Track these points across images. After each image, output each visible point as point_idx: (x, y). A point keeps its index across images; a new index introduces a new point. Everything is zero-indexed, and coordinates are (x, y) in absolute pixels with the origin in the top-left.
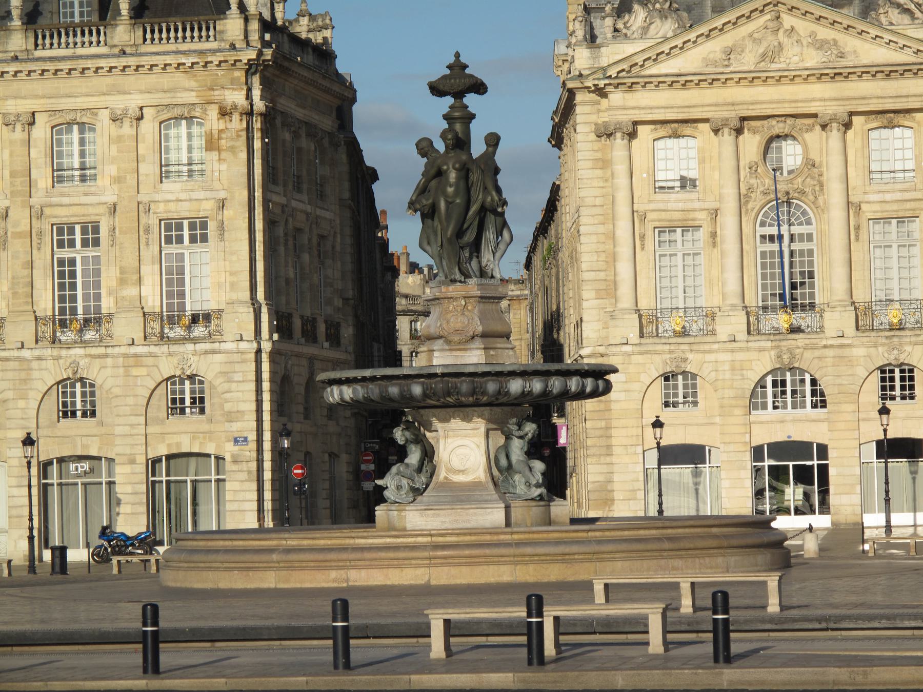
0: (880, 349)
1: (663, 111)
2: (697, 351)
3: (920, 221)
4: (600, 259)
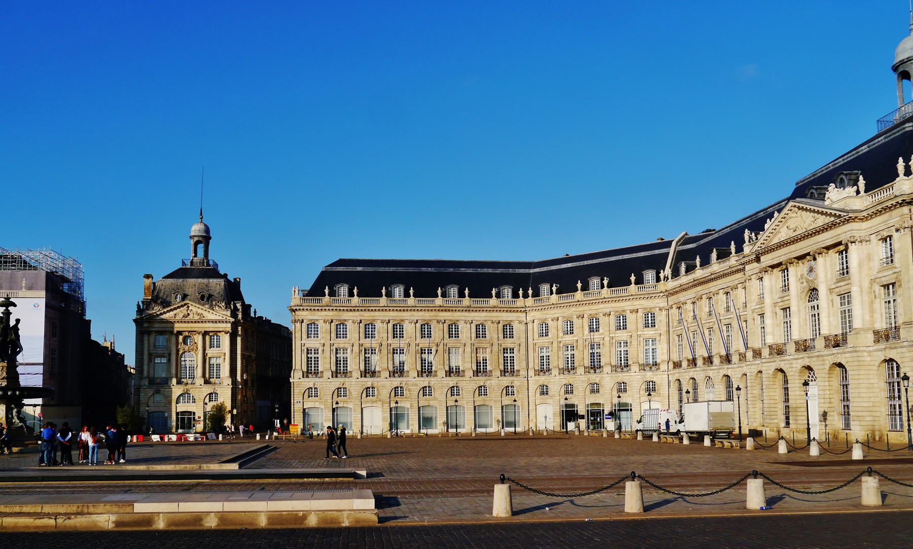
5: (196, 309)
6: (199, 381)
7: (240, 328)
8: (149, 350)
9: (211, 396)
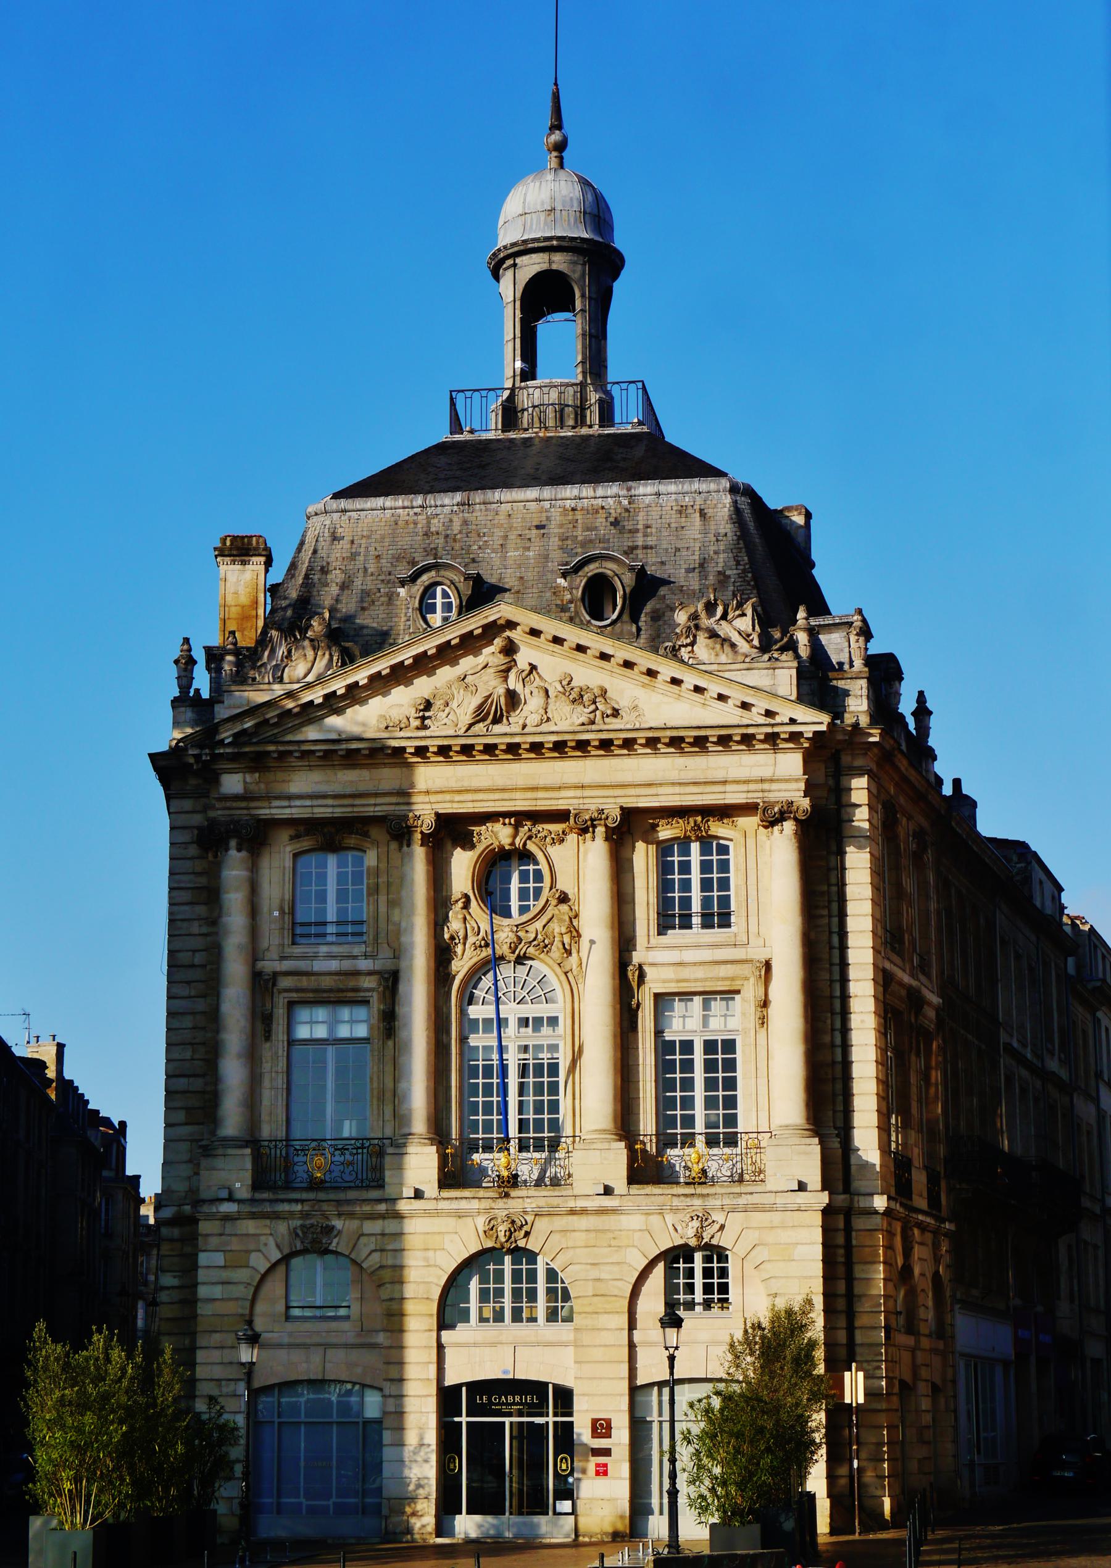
0: (670, 1218)
1: (308, 803)
2: (351, 1215)
3: (743, 999)
4: (197, 1056)
5: (563, 666)
6: (595, 1161)
7: (859, 789)
8: (255, 955)
9: (693, 1273)
